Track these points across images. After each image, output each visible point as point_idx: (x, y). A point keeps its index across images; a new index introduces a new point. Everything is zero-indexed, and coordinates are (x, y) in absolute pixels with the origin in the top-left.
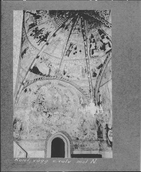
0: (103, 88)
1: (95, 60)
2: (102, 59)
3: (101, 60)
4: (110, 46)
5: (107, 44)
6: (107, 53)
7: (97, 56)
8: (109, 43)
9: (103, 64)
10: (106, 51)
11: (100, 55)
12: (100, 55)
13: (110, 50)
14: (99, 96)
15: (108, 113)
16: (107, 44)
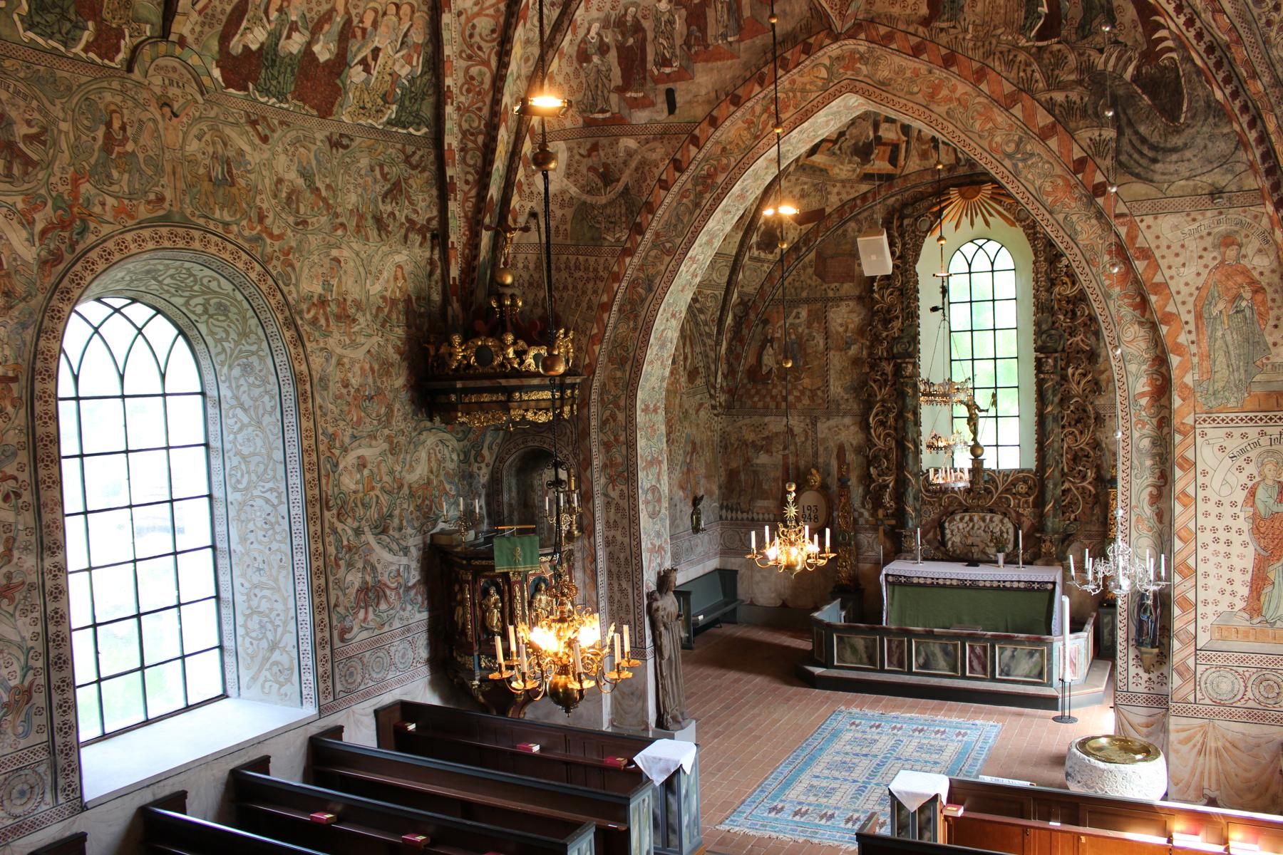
0: (797, 316)
1: (804, 179)
2: (835, 190)
3: (829, 193)
4: (893, 160)
5: (885, 144)
6: (868, 177)
7: (821, 170)
8: (895, 147)
9: (828, 210)
10: (868, 168)
11: (836, 170)
12: (836, 170)
13: (889, 178)
14: (763, 347)
15: (802, 425)
16: (885, 144)
